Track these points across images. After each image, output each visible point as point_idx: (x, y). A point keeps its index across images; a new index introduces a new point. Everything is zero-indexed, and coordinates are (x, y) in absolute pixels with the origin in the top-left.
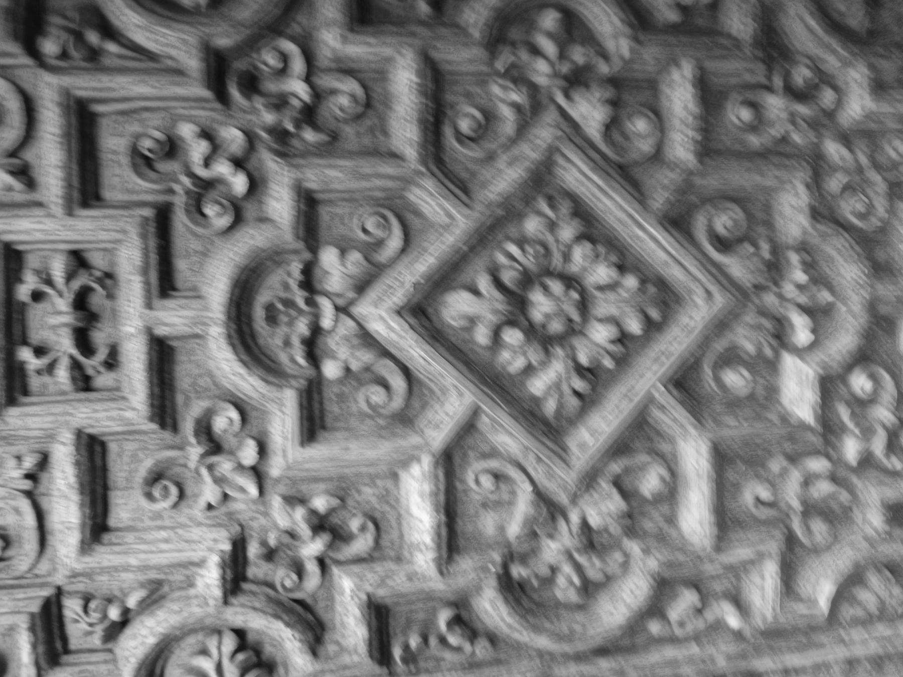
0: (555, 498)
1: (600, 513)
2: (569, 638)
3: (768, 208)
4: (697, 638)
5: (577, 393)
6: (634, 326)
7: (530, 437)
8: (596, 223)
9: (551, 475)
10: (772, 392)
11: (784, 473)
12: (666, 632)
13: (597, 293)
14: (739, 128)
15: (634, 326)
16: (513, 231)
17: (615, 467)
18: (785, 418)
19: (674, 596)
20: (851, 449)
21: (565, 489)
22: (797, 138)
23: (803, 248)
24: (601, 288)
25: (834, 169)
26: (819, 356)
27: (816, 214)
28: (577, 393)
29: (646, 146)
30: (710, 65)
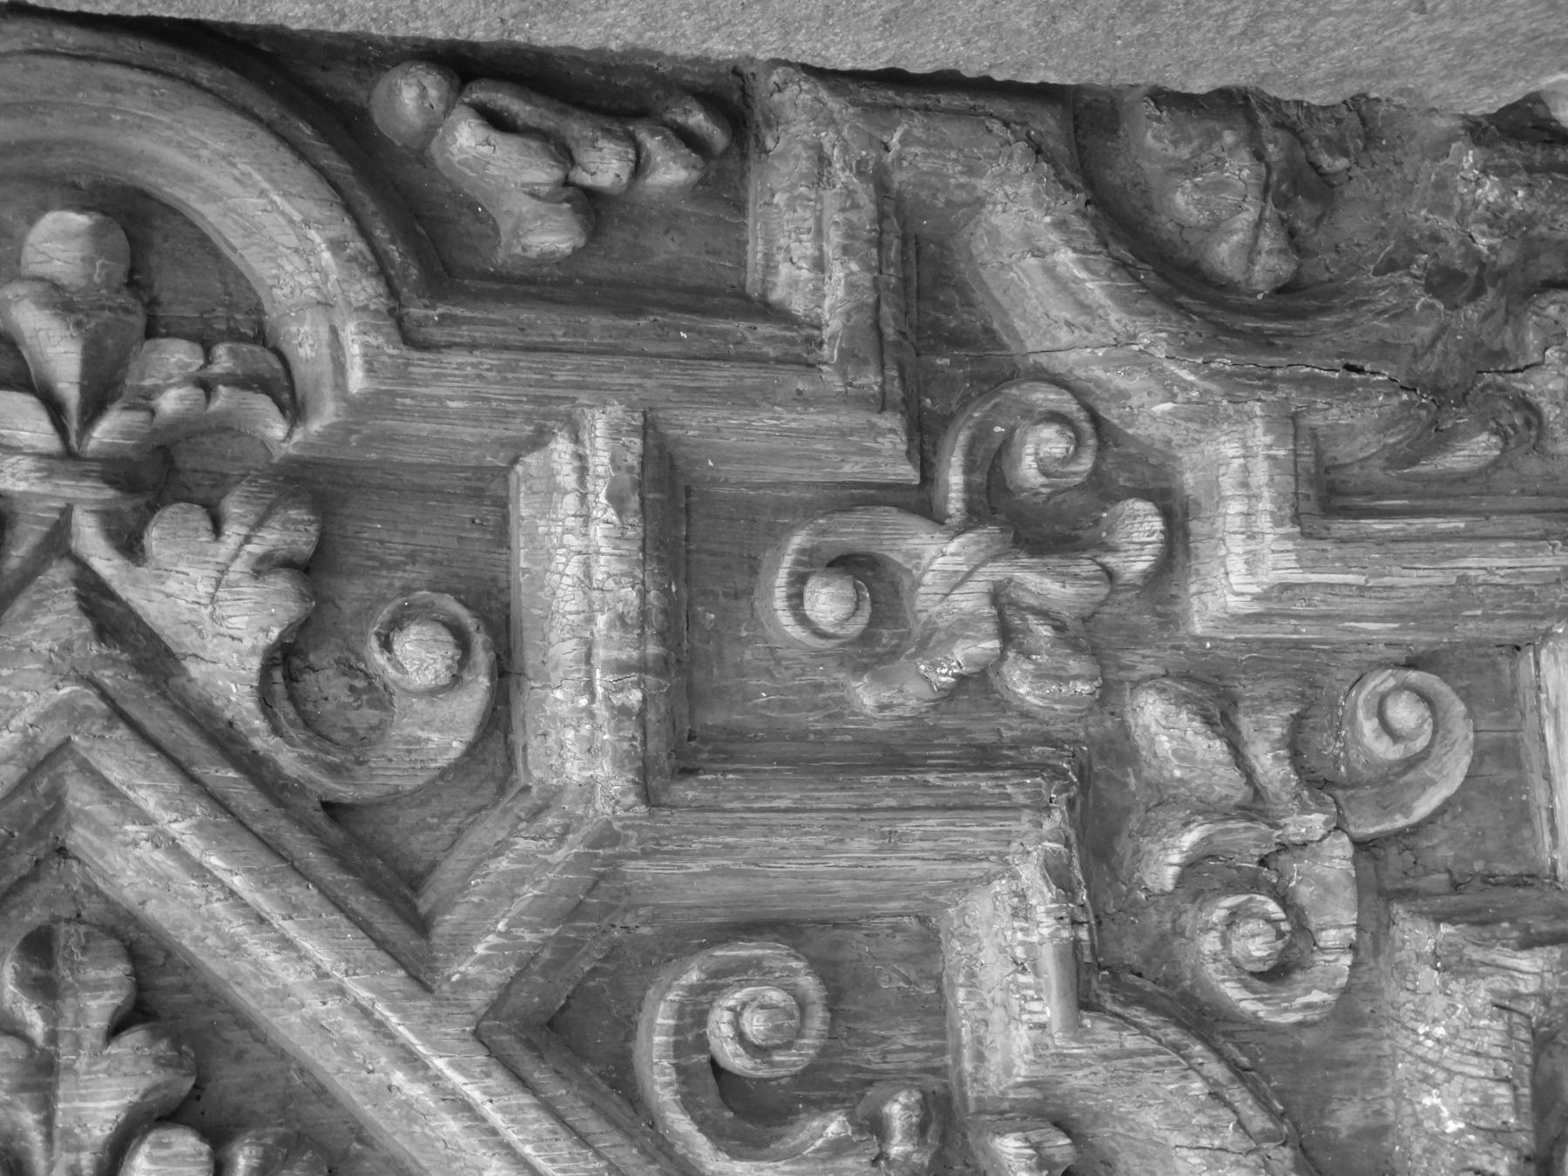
8: (236, 1035)
22: (1021, 684)
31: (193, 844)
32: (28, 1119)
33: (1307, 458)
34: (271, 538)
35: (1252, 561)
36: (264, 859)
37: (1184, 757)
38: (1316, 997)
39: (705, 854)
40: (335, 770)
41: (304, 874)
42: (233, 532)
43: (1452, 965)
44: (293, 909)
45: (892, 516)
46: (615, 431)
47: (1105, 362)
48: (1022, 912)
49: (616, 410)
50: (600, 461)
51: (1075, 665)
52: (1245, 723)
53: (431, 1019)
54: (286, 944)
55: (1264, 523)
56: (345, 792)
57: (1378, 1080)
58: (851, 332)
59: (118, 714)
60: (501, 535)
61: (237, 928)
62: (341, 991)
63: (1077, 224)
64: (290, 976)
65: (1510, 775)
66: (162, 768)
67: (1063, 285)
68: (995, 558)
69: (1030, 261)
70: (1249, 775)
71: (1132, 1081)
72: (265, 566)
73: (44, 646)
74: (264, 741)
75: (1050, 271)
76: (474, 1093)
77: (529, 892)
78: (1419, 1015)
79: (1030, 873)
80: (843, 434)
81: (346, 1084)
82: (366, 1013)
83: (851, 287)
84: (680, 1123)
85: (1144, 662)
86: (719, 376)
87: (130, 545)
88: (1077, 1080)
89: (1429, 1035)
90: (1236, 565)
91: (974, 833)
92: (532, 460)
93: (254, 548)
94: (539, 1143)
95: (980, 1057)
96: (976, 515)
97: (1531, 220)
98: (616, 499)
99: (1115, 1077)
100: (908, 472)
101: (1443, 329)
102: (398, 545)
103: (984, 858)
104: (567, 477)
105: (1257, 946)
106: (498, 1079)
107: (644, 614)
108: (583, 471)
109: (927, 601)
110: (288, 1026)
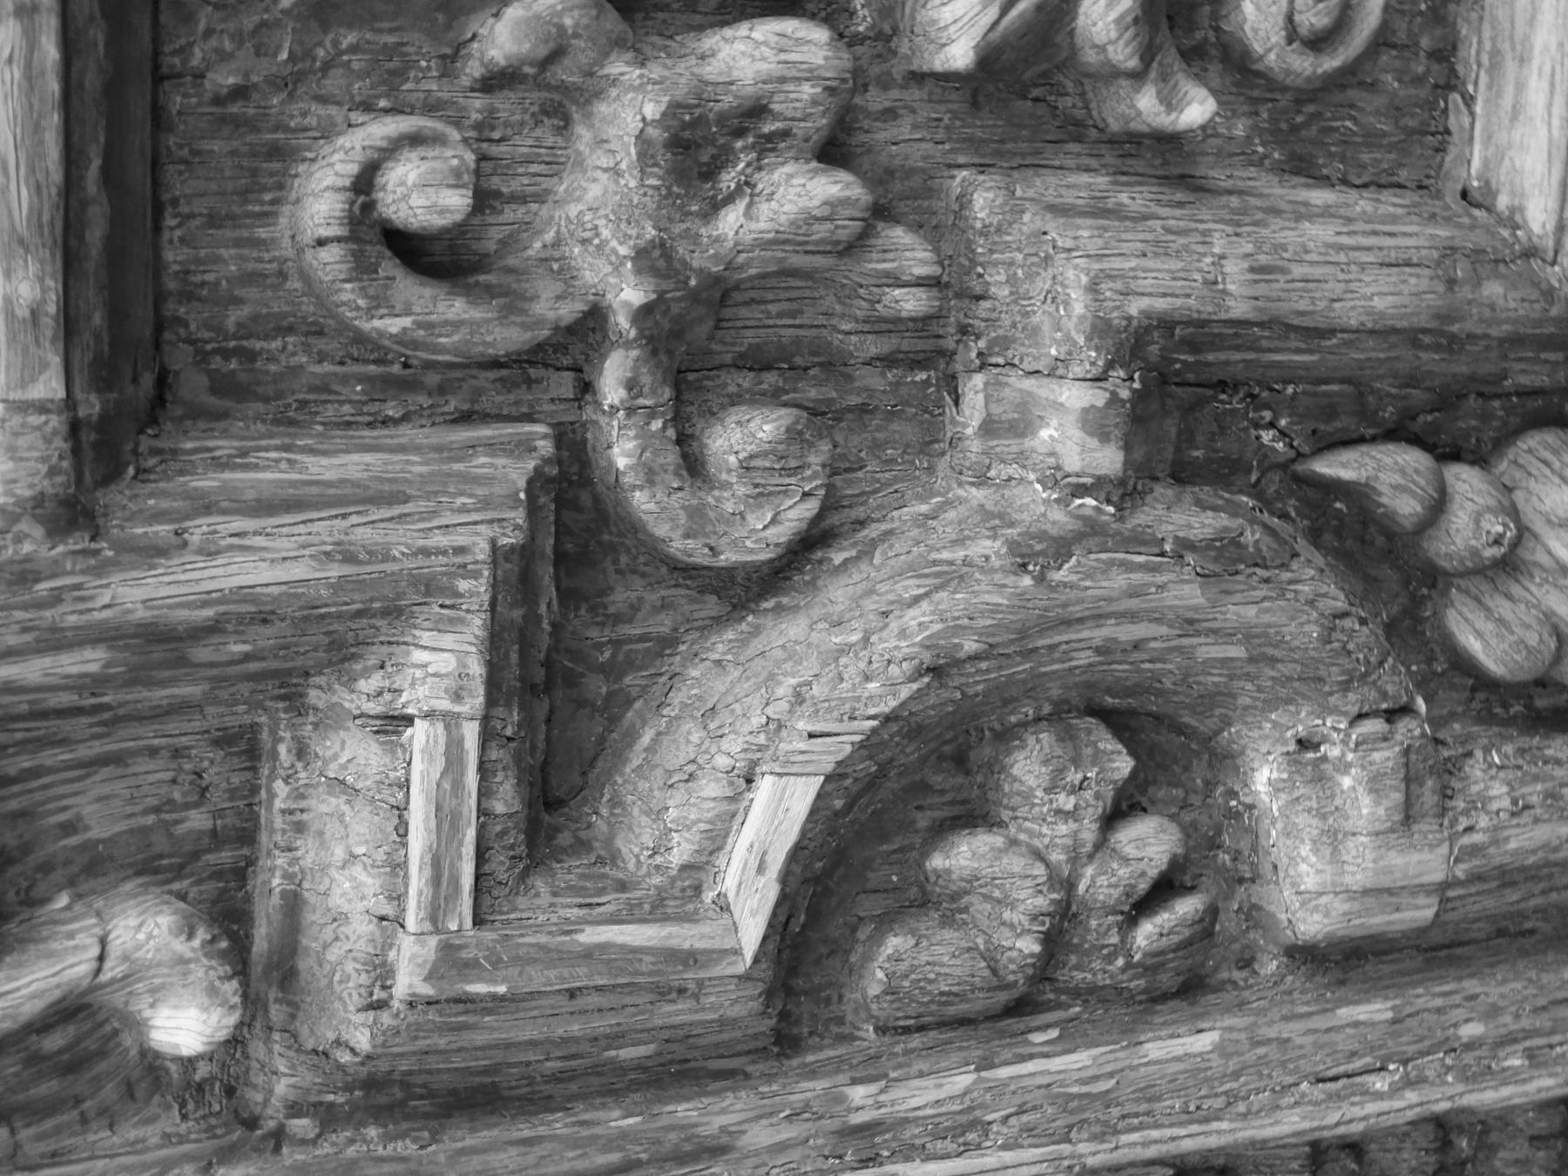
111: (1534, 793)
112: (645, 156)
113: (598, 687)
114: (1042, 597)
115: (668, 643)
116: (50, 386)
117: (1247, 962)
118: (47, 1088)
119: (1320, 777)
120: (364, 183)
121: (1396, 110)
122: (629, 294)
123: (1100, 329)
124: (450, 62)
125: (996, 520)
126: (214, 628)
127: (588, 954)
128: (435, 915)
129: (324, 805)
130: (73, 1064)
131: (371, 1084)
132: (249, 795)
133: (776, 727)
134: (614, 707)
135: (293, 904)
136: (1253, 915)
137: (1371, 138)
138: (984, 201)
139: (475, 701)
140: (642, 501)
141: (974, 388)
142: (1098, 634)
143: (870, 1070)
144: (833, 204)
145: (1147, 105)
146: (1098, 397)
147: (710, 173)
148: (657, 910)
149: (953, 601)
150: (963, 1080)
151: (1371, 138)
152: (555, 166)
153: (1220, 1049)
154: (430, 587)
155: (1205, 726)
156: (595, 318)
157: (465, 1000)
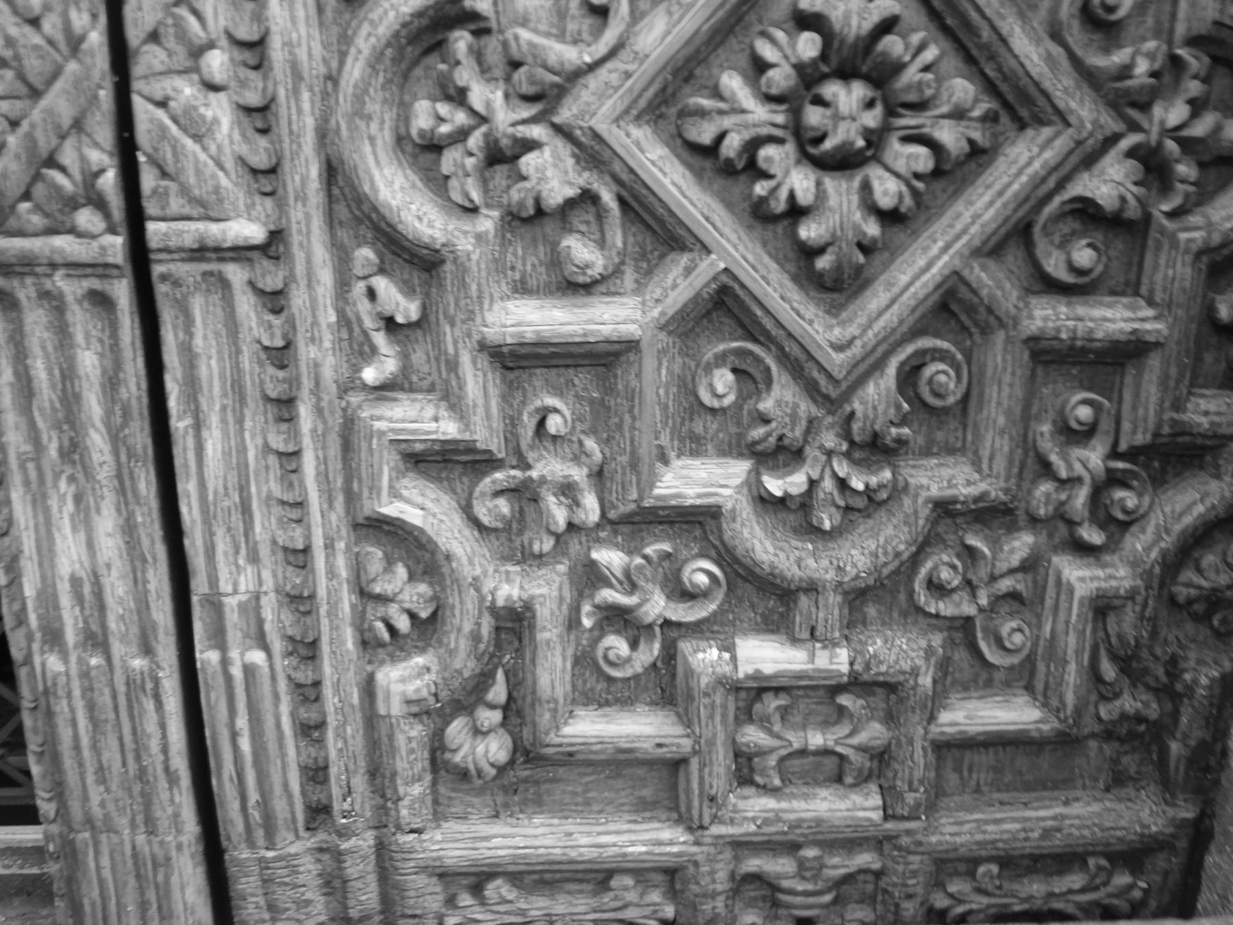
0: (568, 100)
1: (541, 170)
2: (359, 112)
3: (951, 451)
4: (345, 321)
5: (721, 137)
6: (809, 231)
7: (661, 62)
8: (951, 189)
9: (601, 97)
10: (694, 446)
11: (579, 456)
12: (359, 270)
13: (856, 182)
14: (1063, 407)
15: (809, 231)
16: (953, 62)
17: (608, 197)
18: (664, 460)
19: (408, 290)
20: (610, 558)
21: (582, 115)
23: (898, 490)
24: (866, 187)
25: (995, 544)
26: (746, 510)
27: (944, 509)
28: (721, 137)
29: (1054, 265)
30: (1154, 362)
31: (1030, 171)
32: (945, 109)
33: (1117, 602)
34: (1132, 202)
35: (1082, 579)
36: (1023, 195)
37: (1012, 551)
38: (923, 598)
39: (1004, 360)
40: (1044, 227)
41: (1015, 210)
42: (1134, 189)
43: (929, 652)
44: (1005, 205)
45: (1110, 440)
46: (1158, 331)
47: (1157, 526)
48: (969, 483)
49: (1166, 332)
50: (1148, 326)
51: (1051, 508)
52: (1020, 576)
53: (962, 256)
54: (991, 203)
55: (1095, 584)
56: (1037, 229)
57: (884, 624)
58: (1183, 423)
59: (1079, 143)
60: (1113, 293)
61: (997, 187)
62: (973, 223)
63: (1214, 513)
64: (980, 204)
65: (981, 683)
66: (1059, 159)
67: (1189, 508)
68: (1093, 479)
69: (1198, 496)
70: (1002, 576)
71: (906, 523)
72: (1123, 199)
73: (1102, 120)
74: (1057, 200)
75: (1194, 503)
76: (935, 270)
77: (999, 293)
78: (909, 640)
79: (983, 486)
80: (1145, 420)
81: (938, 226)
82: (964, 231)
83: (1199, 425)
84: (910, 349)
85: (1043, 537)
86: (1173, 371)
87: (1131, 153)
88: (907, 501)
89: (902, 642)
90: (1080, 573)
91: (1000, 465)
92: (1143, 303)
93: (1129, 197)
94: (915, 293)
95: (914, 467)
96: (1109, 471)
97: (1191, 698)
98: (1135, 331)
99: (907, 516)
100: (1123, 446)
101: (1156, 657)
102: (1112, 253)
103: (990, 467)
104: (1141, 314)
105: (945, 574)
106: (938, 279)
107: (1092, 340)
108: (1143, 320)
109: (1077, 452)
110: (959, 206)
111: (414, 745)
112: (566, 477)
113: (444, 475)
114: (465, 584)
115: (454, 491)
116: (509, 340)
117: (370, 662)
118: (356, 347)
119: (419, 675)
120: (556, 411)
121: (592, 690)
122: (534, 474)
123: (532, 597)
124: (583, 432)
125: (485, 573)
126: (458, 378)
127: (381, 469)
128: (392, 430)
129: (418, 406)
130: (361, 353)
131: (352, 421)
132: (420, 391)
133: (434, 515)
134: (437, 480)
135: (395, 400)
136: (382, 663)
137: (585, 682)
138: (562, 568)
139: (442, 438)
140: (487, 480)
141: (518, 568)
142: (458, 606)
143: (348, 549)
144: (556, 523)
145: (586, 608)
146: (515, 598)
147: (564, 494)
148: (391, 487)
149: (464, 560)
150: (344, 574)
151: (585, 682)
152: (563, 458)
153: (347, 651)
154: (467, 426)
155: (433, 642)
156: (528, 467)
157: (372, 437)
